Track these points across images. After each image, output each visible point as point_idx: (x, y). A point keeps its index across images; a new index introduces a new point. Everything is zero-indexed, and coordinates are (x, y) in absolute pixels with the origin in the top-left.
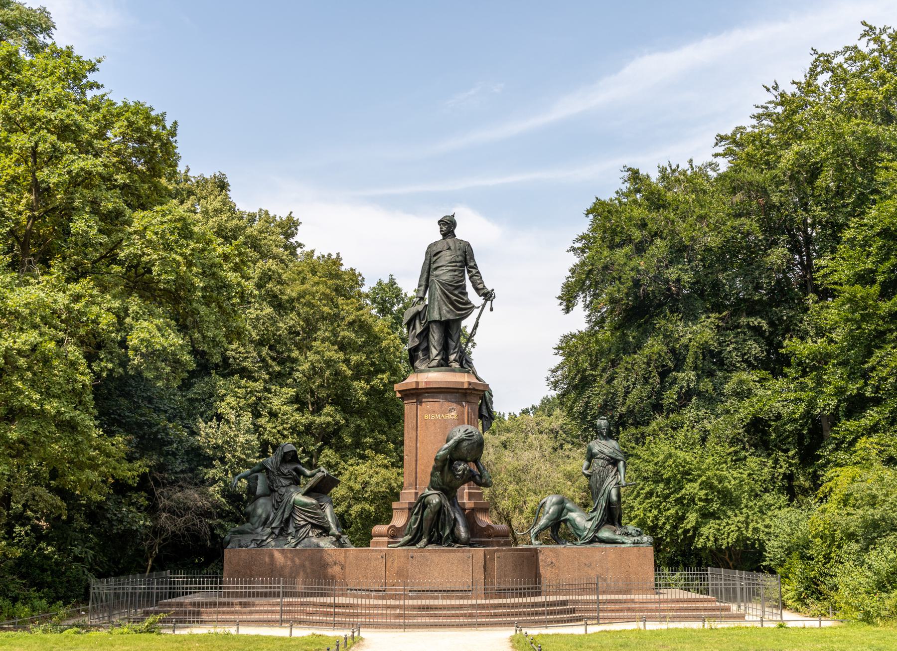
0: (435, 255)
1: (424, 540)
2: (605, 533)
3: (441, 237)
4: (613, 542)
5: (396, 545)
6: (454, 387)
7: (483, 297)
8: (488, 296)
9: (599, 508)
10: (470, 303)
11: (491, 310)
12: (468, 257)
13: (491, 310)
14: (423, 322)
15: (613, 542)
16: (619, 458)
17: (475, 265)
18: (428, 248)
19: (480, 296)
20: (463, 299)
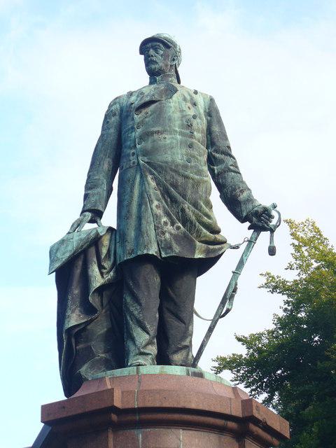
3: (146, 78)
6: (218, 409)
7: (248, 224)
8: (260, 220)
10: (218, 232)
11: (272, 251)
13: (272, 251)
14: (107, 264)
17: (229, 147)
18: (110, 106)
19: (243, 221)
20: (209, 217)
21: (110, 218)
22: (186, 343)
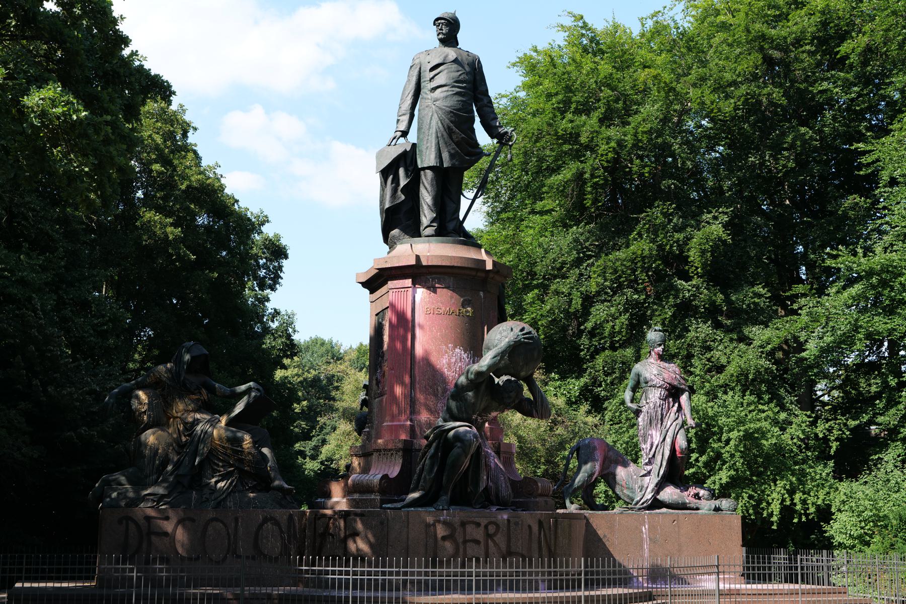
0: (432, 69)
1: (445, 498)
2: (670, 493)
4: (683, 506)
5: (399, 505)
9: (659, 458)
12: (478, 78)
15: (683, 506)
16: (683, 387)
21: (412, 137)
22: (455, 216)
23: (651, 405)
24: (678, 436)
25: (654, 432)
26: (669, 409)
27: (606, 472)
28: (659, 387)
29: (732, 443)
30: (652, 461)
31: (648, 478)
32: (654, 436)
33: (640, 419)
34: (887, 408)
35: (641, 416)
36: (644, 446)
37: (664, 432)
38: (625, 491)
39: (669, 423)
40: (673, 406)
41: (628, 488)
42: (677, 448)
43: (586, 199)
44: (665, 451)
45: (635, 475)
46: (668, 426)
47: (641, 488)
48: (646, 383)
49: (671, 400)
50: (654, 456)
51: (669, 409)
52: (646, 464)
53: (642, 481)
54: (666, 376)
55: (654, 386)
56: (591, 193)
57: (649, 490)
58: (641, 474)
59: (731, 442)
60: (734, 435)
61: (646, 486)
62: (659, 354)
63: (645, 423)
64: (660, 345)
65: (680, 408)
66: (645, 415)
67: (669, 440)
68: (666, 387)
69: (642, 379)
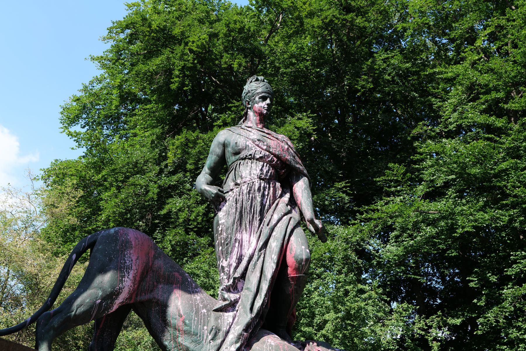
9: (253, 278)
23: (244, 188)
24: (292, 238)
25: (245, 236)
26: (275, 198)
27: (144, 297)
28: (261, 159)
29: (329, 326)
30: (239, 286)
31: (231, 314)
32: (245, 243)
33: (221, 214)
34: (489, 306)
35: (224, 208)
36: (225, 264)
37: (266, 230)
38: (180, 340)
39: (276, 217)
40: (281, 196)
41: (187, 333)
42: (290, 260)
43: (172, 83)
44: (266, 264)
45: (205, 307)
46: (273, 222)
47: (216, 332)
48: (237, 153)
49: (278, 185)
50: (243, 276)
51: (275, 198)
52: (228, 289)
53: (217, 319)
54: (272, 143)
55: (252, 158)
56: (178, 76)
57: (231, 337)
58: (215, 308)
59: (328, 325)
60: (331, 316)
61: (224, 329)
62: (260, 114)
63: (231, 220)
64: (264, 99)
65: (293, 202)
66: (231, 206)
67: (274, 245)
68: (272, 160)
69: (229, 150)
